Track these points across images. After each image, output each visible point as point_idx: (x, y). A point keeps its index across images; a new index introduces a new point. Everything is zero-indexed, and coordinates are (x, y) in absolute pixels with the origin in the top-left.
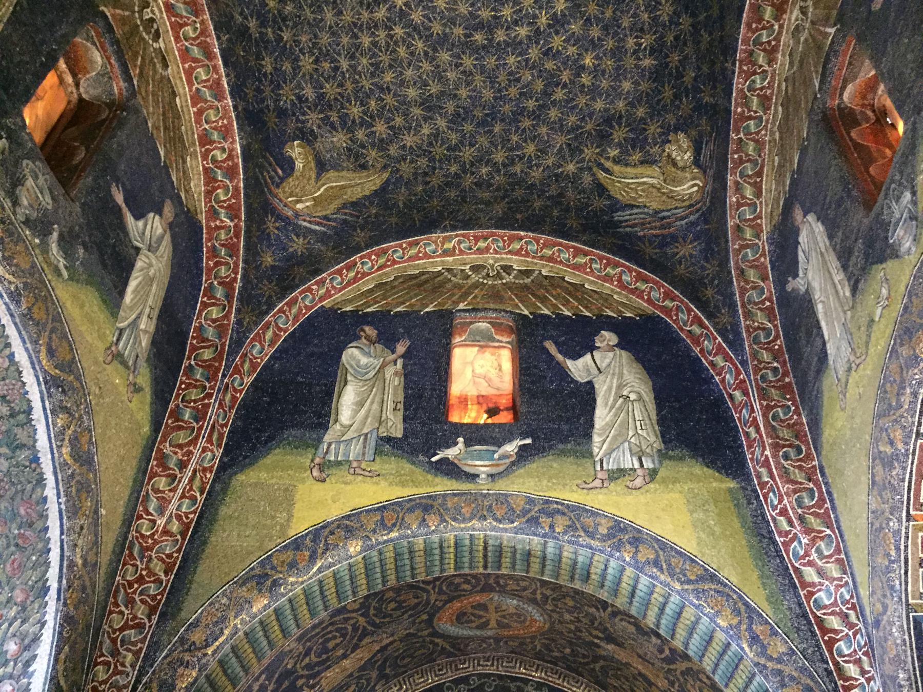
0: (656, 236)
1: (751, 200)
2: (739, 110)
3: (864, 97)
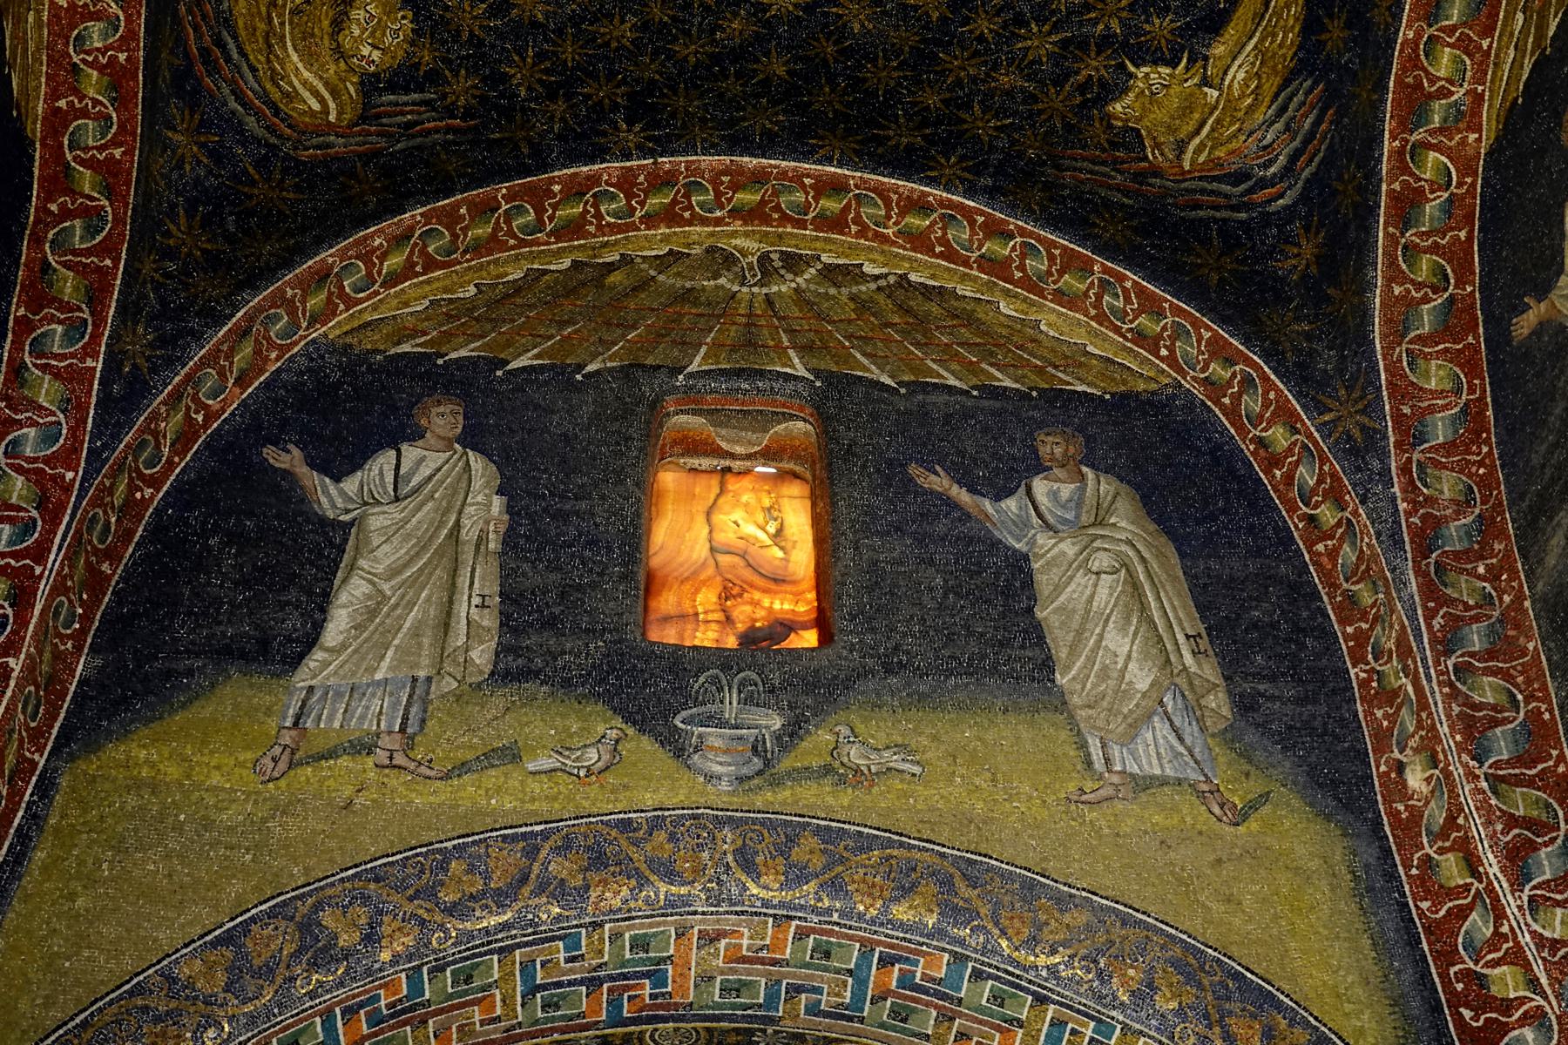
0: (187, 55)
1: (379, 273)
2: (557, 188)
3: (675, 443)
